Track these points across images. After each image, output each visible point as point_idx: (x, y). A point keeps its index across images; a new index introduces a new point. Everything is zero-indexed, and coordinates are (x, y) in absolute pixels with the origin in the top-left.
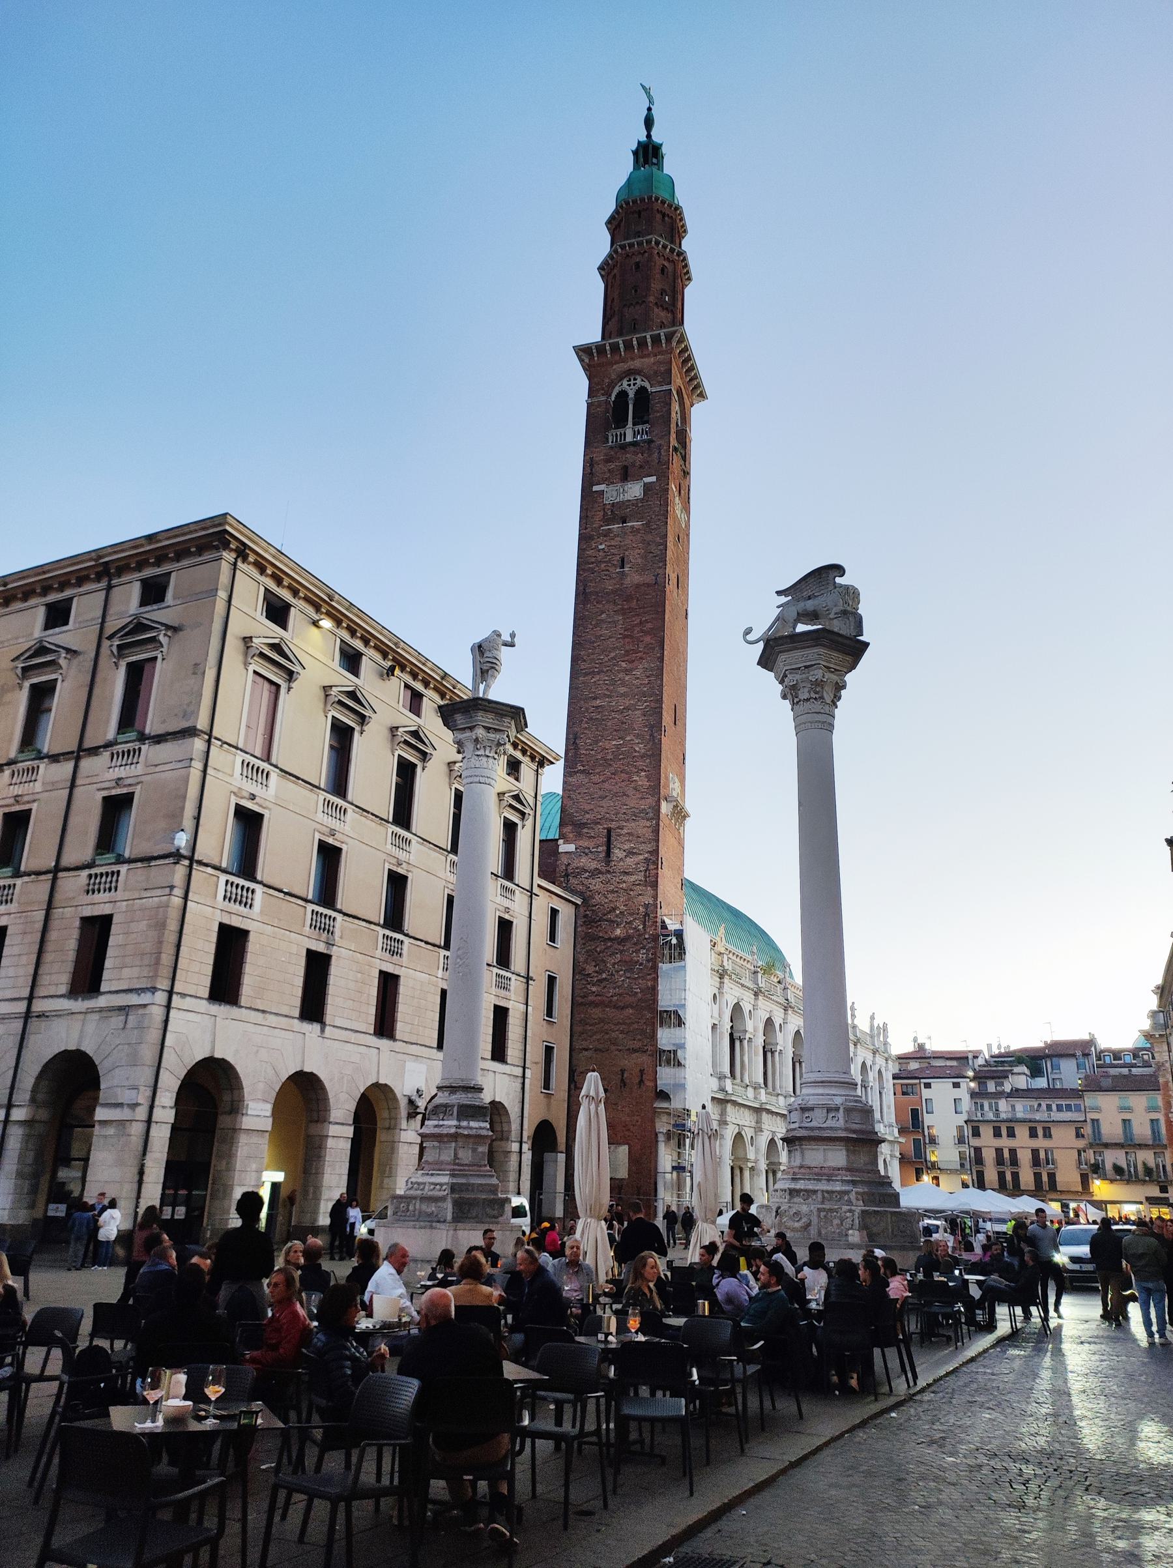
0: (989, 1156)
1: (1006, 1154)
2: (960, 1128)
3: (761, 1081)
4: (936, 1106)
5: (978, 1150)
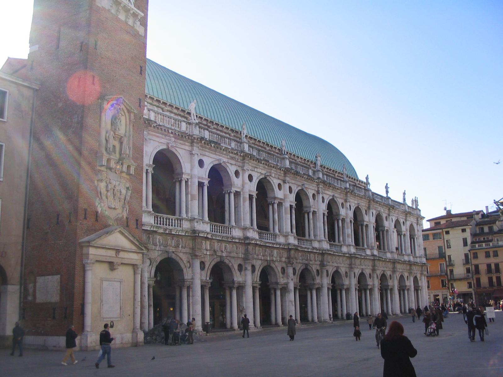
0: (483, 268)
1: (493, 267)
2: (466, 255)
3: (290, 230)
4: (452, 243)
5: (477, 267)
